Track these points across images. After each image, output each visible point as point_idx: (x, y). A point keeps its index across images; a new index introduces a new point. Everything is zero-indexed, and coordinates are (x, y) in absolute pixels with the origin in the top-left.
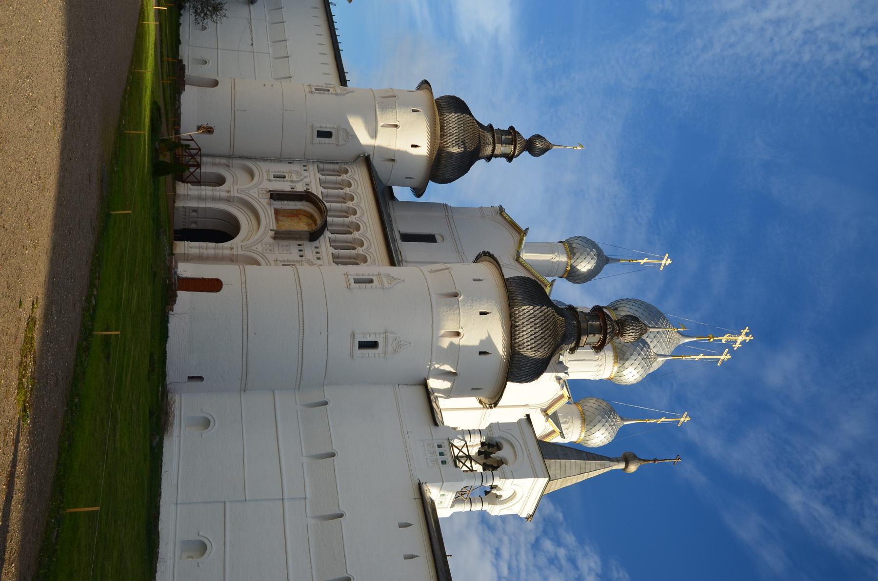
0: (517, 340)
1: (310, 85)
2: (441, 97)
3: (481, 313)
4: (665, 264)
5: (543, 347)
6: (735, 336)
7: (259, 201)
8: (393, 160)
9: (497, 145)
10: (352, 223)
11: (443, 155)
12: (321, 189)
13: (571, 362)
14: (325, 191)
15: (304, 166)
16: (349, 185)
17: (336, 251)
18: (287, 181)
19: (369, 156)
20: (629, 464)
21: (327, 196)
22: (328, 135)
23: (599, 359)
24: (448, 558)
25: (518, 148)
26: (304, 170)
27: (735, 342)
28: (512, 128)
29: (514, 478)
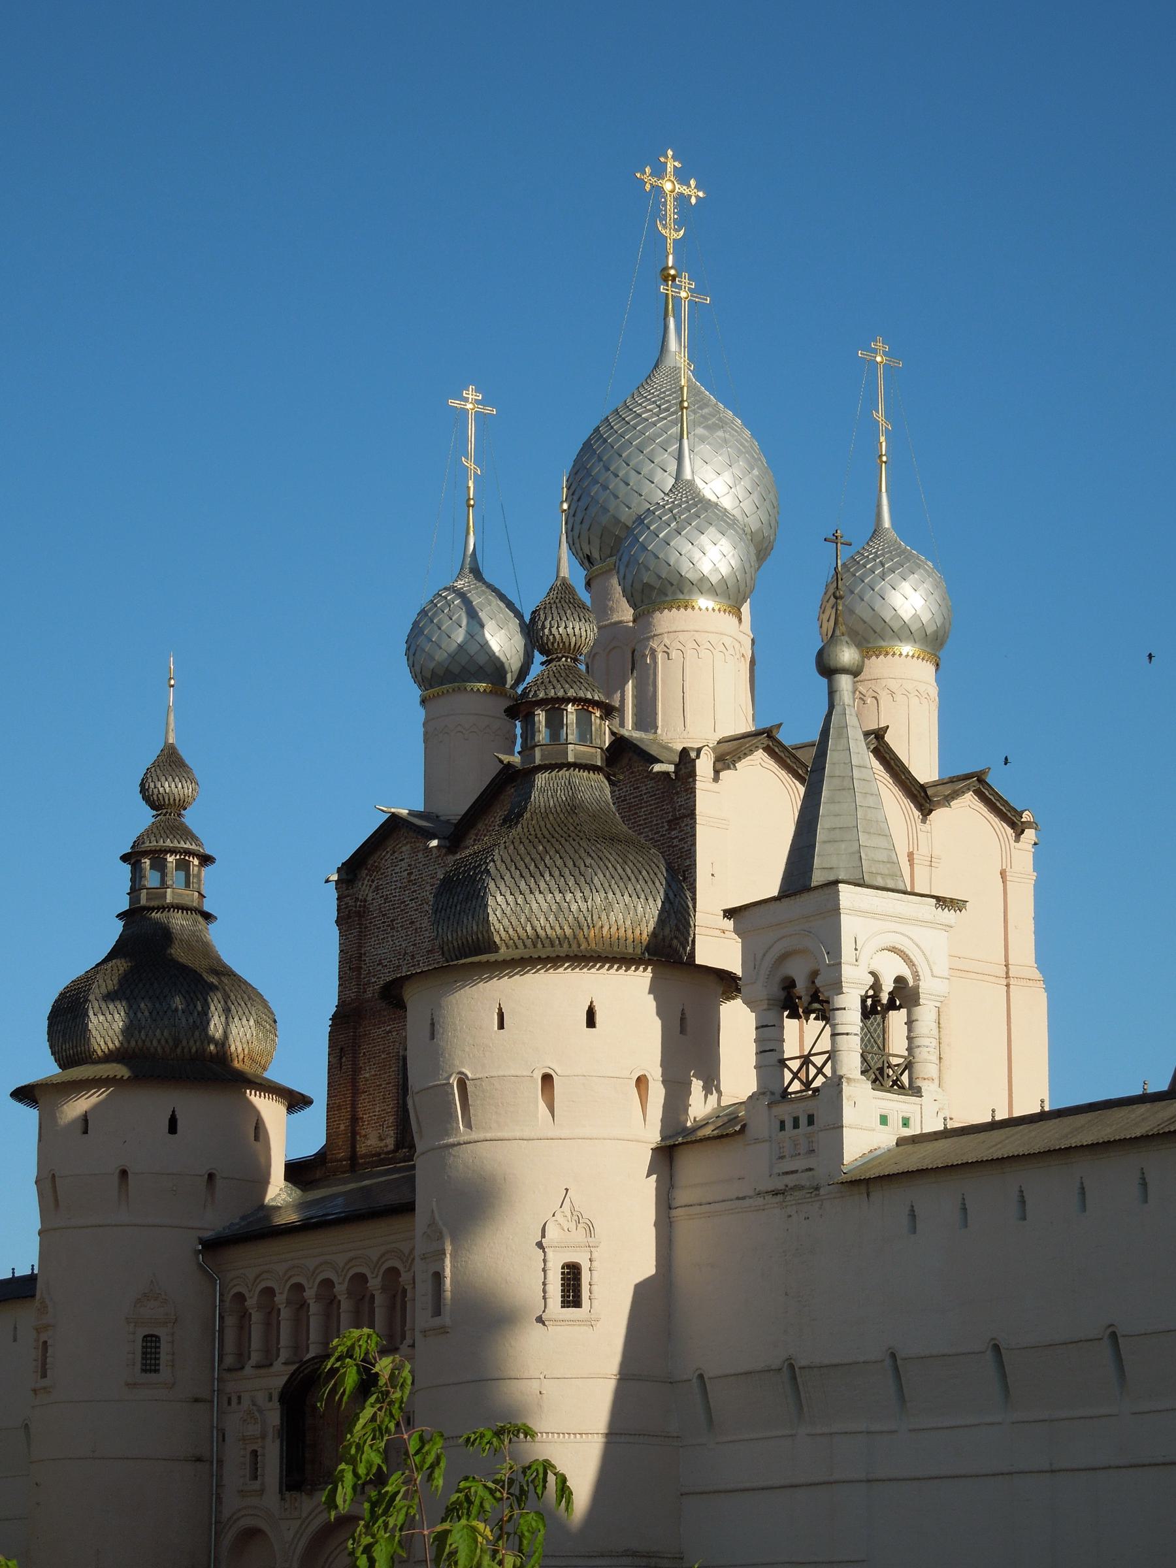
0: (568, 931)
1: (35, 1391)
2: (53, 1054)
3: (501, 1026)
4: (477, 401)
5: (583, 868)
6: (665, 204)
7: (307, 1517)
8: (211, 1176)
9: (168, 901)
10: (350, 1293)
11: (194, 1050)
12: (278, 1366)
13: (688, 722)
14: (284, 1355)
15: (229, 1403)
16: (269, 1292)
17: (408, 1341)
18: (263, 1447)
19: (201, 1241)
20: (839, 666)
21: (298, 1346)
22: (151, 1343)
23: (681, 647)
24: (998, 1118)
25: (176, 844)
26: (239, 1403)
27: (682, 199)
28: (125, 858)
29: (840, 963)
